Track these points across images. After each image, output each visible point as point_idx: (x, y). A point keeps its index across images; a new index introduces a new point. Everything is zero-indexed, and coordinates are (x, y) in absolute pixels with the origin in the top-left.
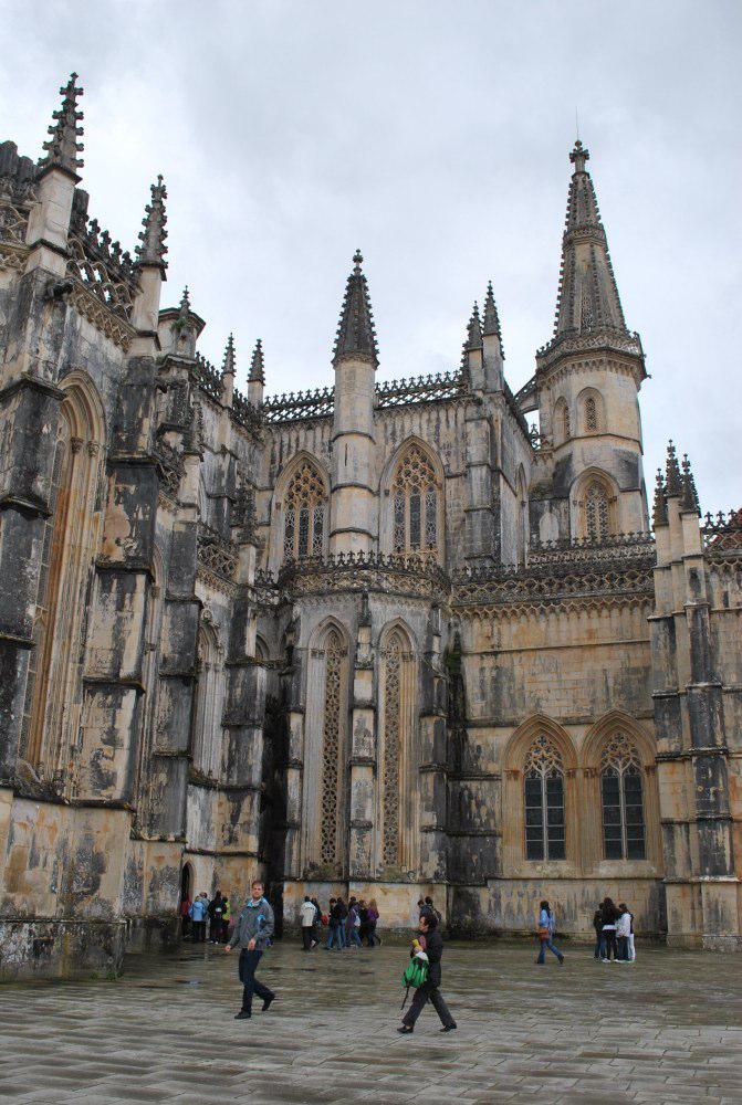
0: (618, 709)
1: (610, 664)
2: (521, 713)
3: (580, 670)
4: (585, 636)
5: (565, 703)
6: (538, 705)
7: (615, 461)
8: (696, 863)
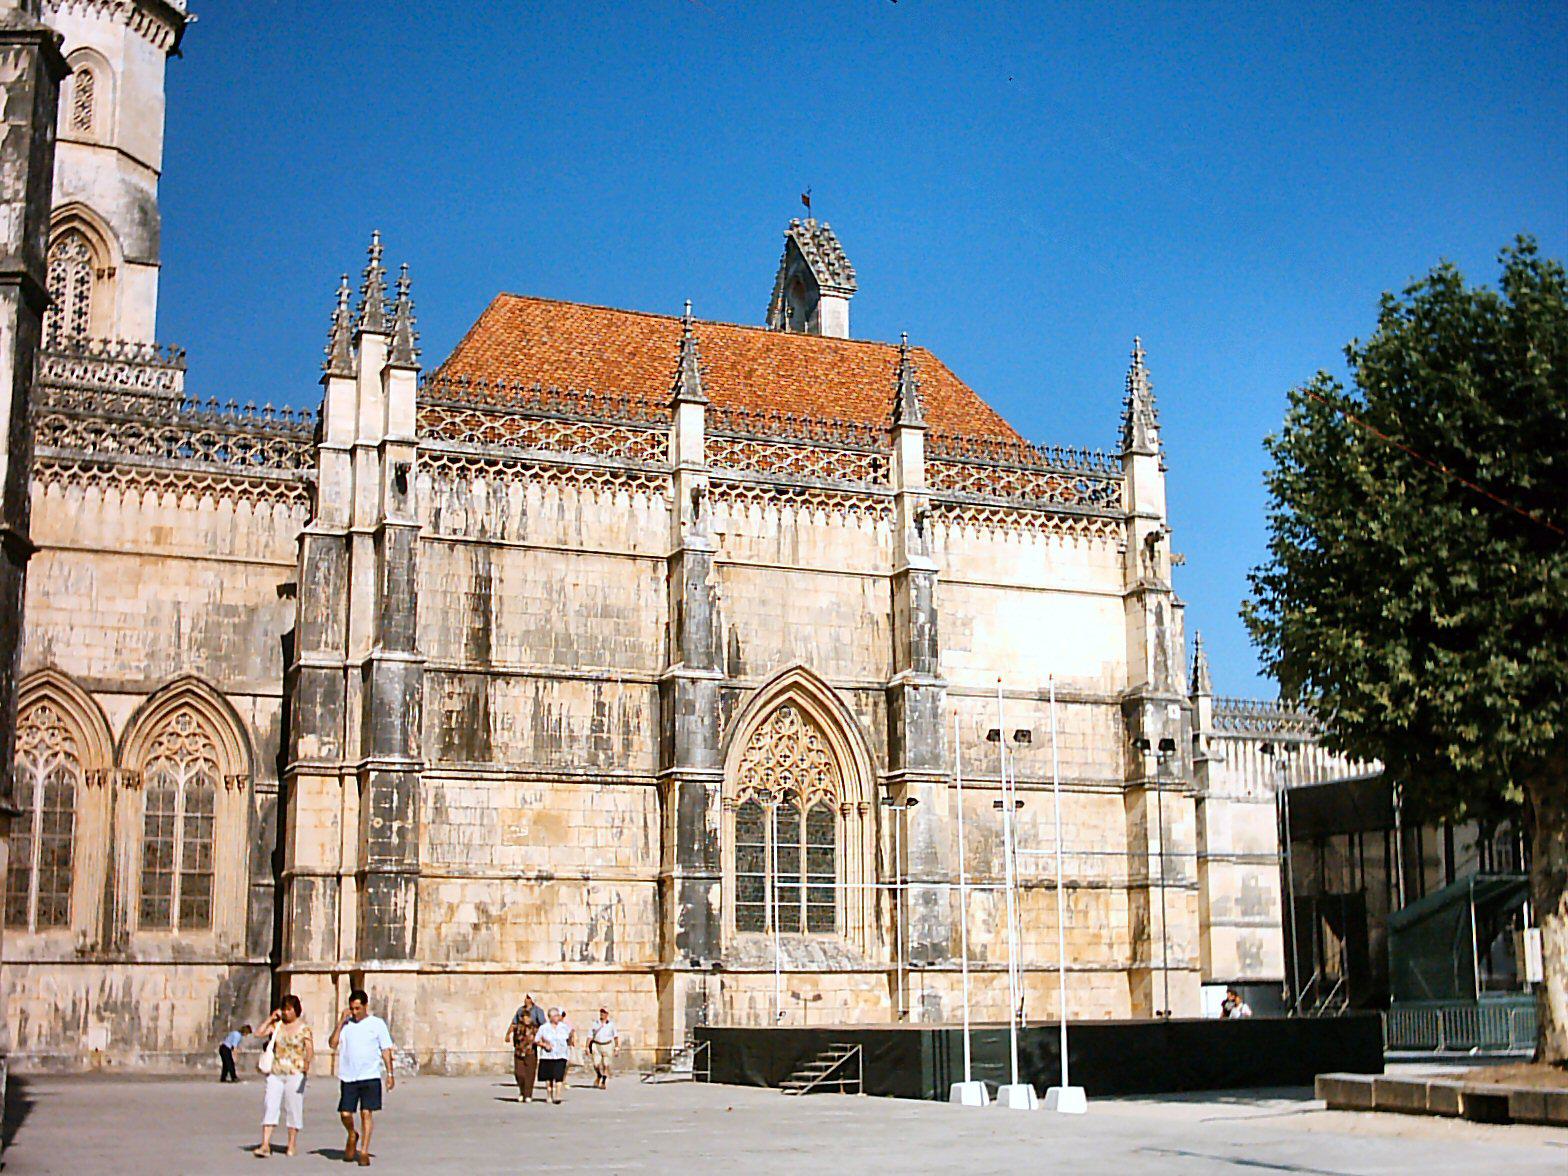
1: (190, 592)
4: (149, 537)
5: (98, 652)
6: (48, 650)
7: (124, 201)
8: (349, 941)
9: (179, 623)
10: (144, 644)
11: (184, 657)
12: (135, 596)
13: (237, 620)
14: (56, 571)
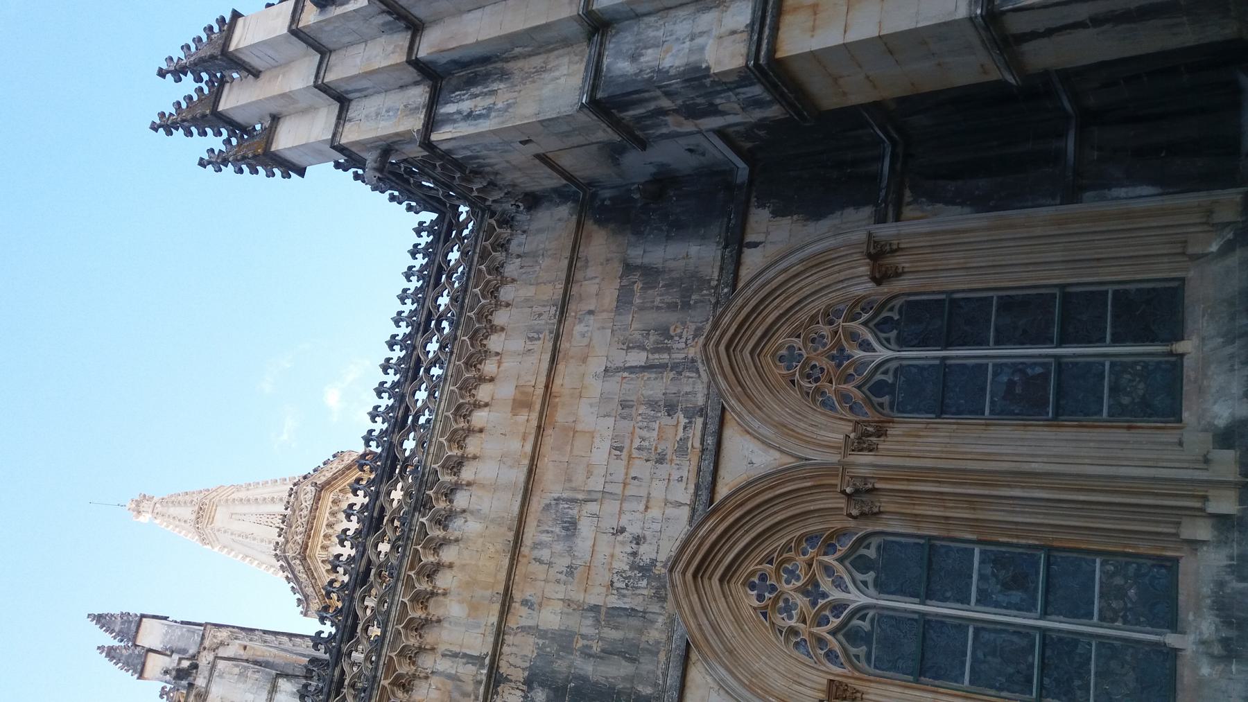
0: (701, 340)
2: (655, 634)
3: (592, 435)
4: (522, 418)
5: (658, 490)
6: (645, 570)
9: (631, 369)
10: (654, 419)
11: (678, 357)
12: (592, 435)
13: (638, 286)
14: (545, 554)
